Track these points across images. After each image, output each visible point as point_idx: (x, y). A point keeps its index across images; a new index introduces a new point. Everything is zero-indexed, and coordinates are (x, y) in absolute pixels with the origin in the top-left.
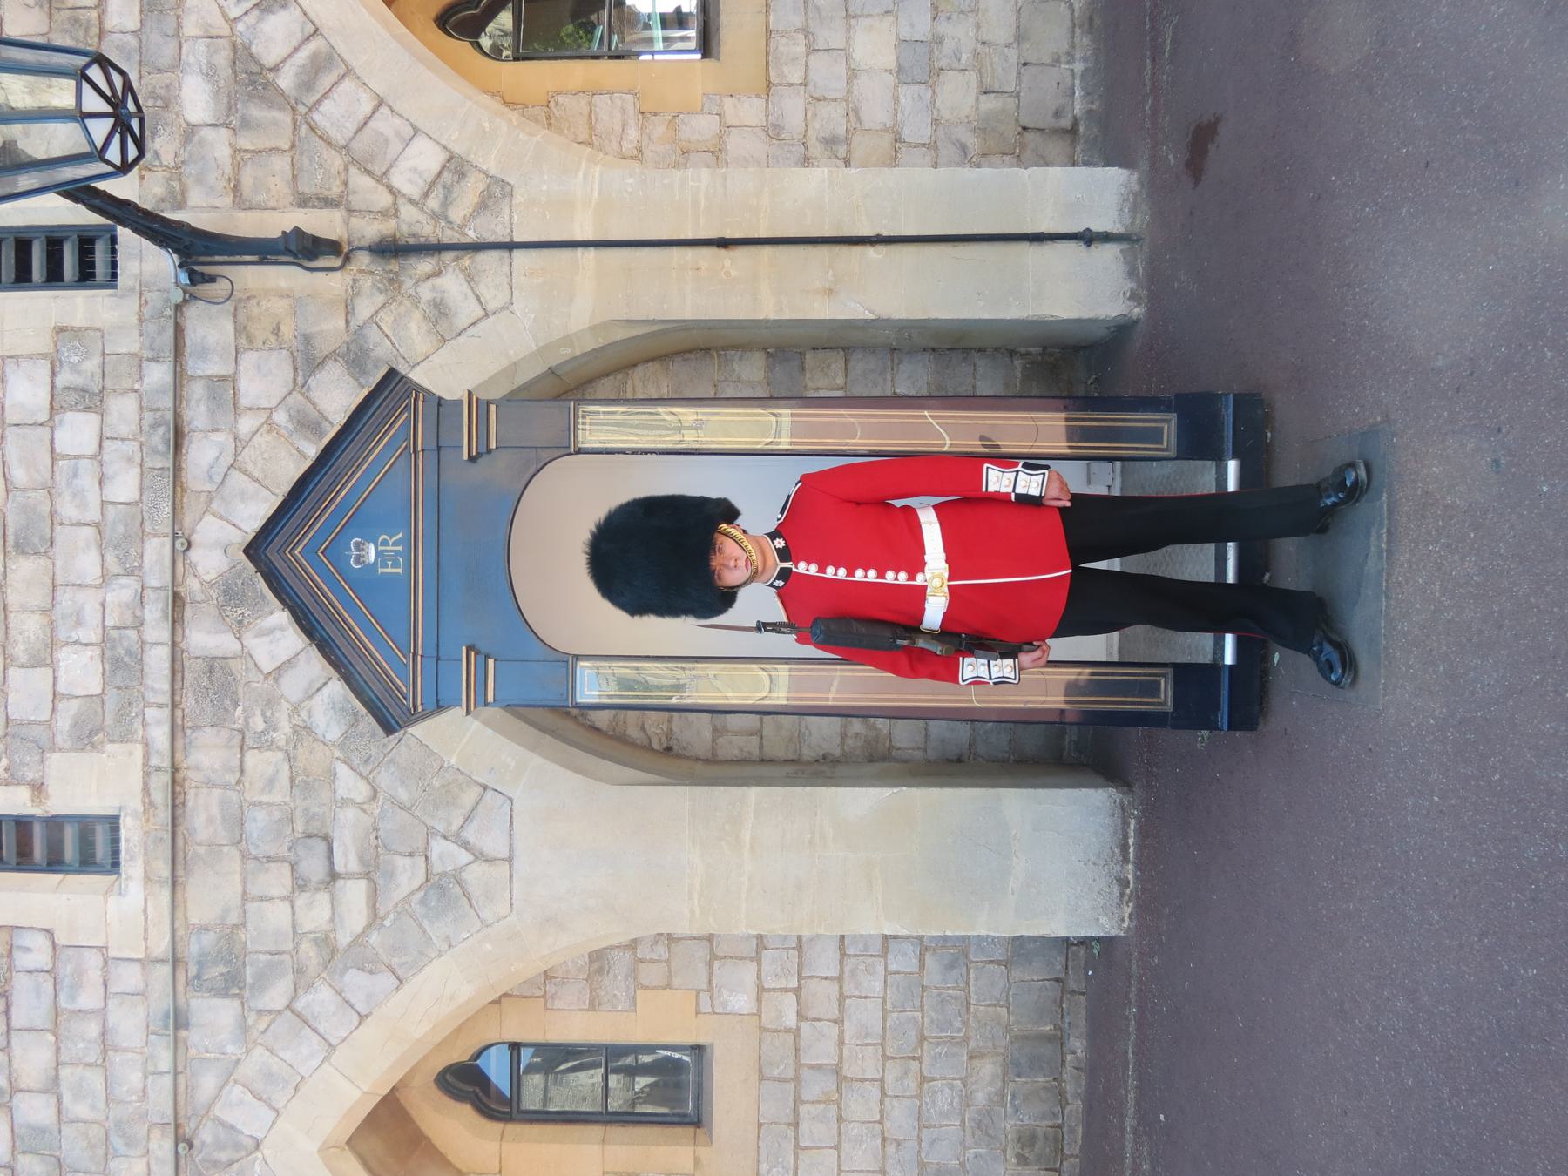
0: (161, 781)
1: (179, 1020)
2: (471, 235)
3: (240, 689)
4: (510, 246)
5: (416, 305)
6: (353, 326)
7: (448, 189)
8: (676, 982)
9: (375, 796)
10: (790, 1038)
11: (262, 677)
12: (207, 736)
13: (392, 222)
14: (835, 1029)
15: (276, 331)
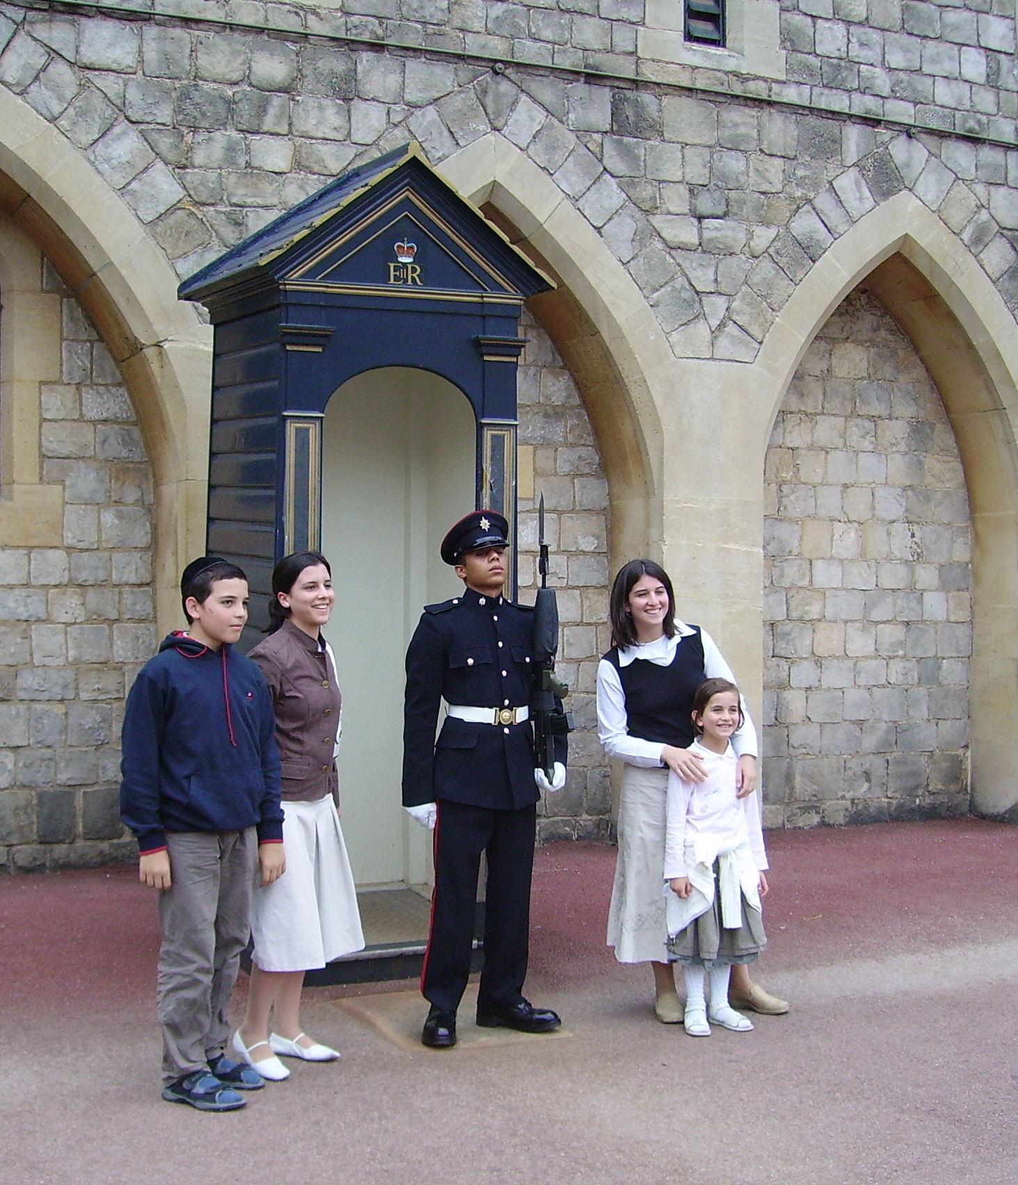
0: (756, 89)
8: (540, 481)
11: (830, 179)
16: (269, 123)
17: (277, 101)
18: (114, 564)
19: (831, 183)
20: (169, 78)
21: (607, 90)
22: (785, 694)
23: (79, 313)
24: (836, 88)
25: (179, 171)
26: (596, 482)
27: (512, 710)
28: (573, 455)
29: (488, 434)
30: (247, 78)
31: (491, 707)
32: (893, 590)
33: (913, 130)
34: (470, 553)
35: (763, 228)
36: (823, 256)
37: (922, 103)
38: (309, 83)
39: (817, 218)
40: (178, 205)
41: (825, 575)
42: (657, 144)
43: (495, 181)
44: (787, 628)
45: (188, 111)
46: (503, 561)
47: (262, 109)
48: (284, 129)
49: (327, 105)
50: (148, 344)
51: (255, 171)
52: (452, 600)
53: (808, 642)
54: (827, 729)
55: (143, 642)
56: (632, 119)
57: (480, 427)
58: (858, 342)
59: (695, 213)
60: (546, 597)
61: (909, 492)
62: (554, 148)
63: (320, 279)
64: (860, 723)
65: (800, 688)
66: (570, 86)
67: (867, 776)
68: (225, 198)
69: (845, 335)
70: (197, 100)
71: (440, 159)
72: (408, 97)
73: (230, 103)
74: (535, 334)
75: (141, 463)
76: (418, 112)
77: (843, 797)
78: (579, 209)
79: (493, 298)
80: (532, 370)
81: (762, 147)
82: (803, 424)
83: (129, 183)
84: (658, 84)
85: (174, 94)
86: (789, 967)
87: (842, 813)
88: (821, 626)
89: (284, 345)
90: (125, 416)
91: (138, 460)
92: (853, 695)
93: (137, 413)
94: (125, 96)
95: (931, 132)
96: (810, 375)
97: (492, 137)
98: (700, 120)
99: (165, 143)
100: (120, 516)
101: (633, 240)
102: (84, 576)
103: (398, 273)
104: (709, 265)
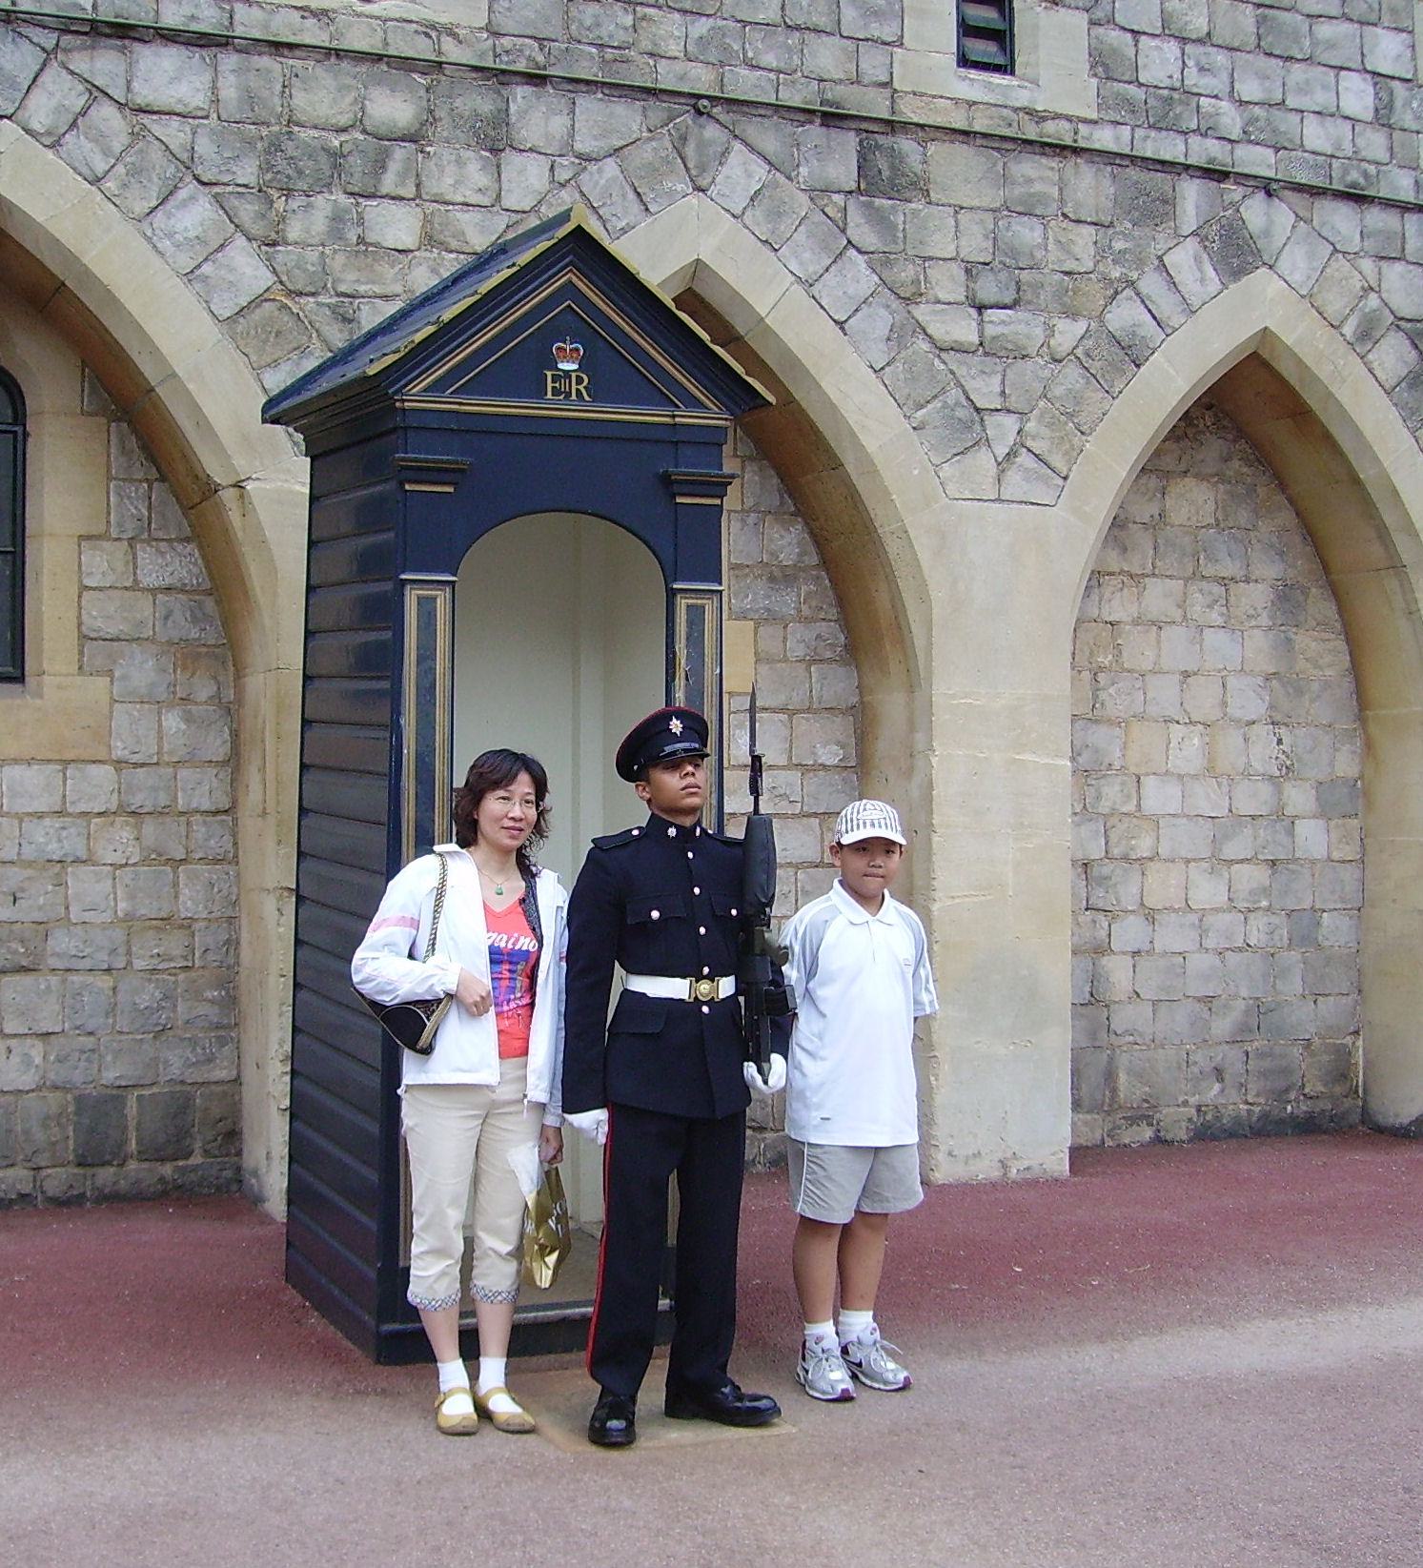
1: (833, 118)
8: (764, 669)
11: (1160, 253)
16: (388, 183)
17: (400, 153)
18: (179, 785)
19: (1160, 258)
20: (254, 124)
21: (852, 134)
22: (1104, 960)
23: (133, 442)
24: (1167, 130)
25: (267, 248)
26: (841, 671)
27: (713, 981)
28: (809, 633)
29: (682, 603)
30: (359, 123)
31: (684, 977)
32: (1253, 817)
33: (1275, 186)
34: (655, 766)
35: (1068, 321)
36: (1151, 359)
37: (1286, 148)
38: (444, 129)
39: (1142, 307)
40: (266, 296)
41: (1159, 797)
42: (921, 207)
43: (698, 260)
44: (1106, 870)
45: (279, 168)
46: (703, 776)
47: (380, 165)
48: (409, 191)
49: (469, 159)
50: (224, 484)
51: (370, 249)
52: (631, 830)
53: (1135, 890)
54: (1163, 1008)
55: (220, 891)
56: (886, 174)
57: (671, 594)
58: (1201, 477)
59: (974, 301)
60: (758, 825)
61: (1274, 682)
62: (779, 215)
63: (452, 393)
64: (1208, 999)
65: (1124, 953)
66: (800, 129)
67: (1219, 1073)
68: (329, 285)
69: (1182, 467)
70: (290, 152)
71: (624, 231)
72: (578, 147)
73: (337, 157)
74: (756, 469)
75: (218, 646)
76: (592, 167)
77: (1185, 1103)
78: (813, 297)
79: (687, 418)
80: (753, 518)
81: (1066, 210)
82: (1126, 590)
83: (199, 266)
84: (922, 126)
85: (259, 145)
86: (1101, 1339)
87: (1184, 1124)
89: (401, 484)
90: (195, 582)
91: (213, 642)
92: (1199, 962)
93: (212, 579)
94: (193, 148)
95: (1299, 188)
96: (1135, 523)
97: (694, 200)
98: (980, 175)
99: (247, 210)
100: (188, 719)
101: (889, 339)
102: (136, 801)
103: (557, 385)
104: (994, 372)
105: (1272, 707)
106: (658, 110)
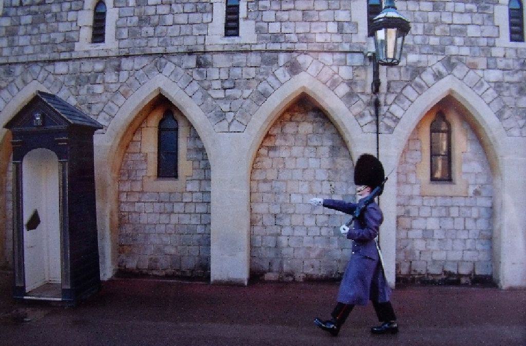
0: (248, 47)
1: (190, 53)
2: (381, 124)
3: (270, 66)
4: (378, 133)
5: (364, 110)
6: (359, 95)
7: (391, 118)
9: (244, 99)
10: (180, 200)
12: (259, 59)
13: (384, 104)
14: (182, 211)
15: (357, 76)
38: (108, 69)
41: (295, 198)
73: (88, 78)
88: (293, 216)
92: (306, 239)
99: (73, 90)
105: (329, 177)
106: (151, 58)
